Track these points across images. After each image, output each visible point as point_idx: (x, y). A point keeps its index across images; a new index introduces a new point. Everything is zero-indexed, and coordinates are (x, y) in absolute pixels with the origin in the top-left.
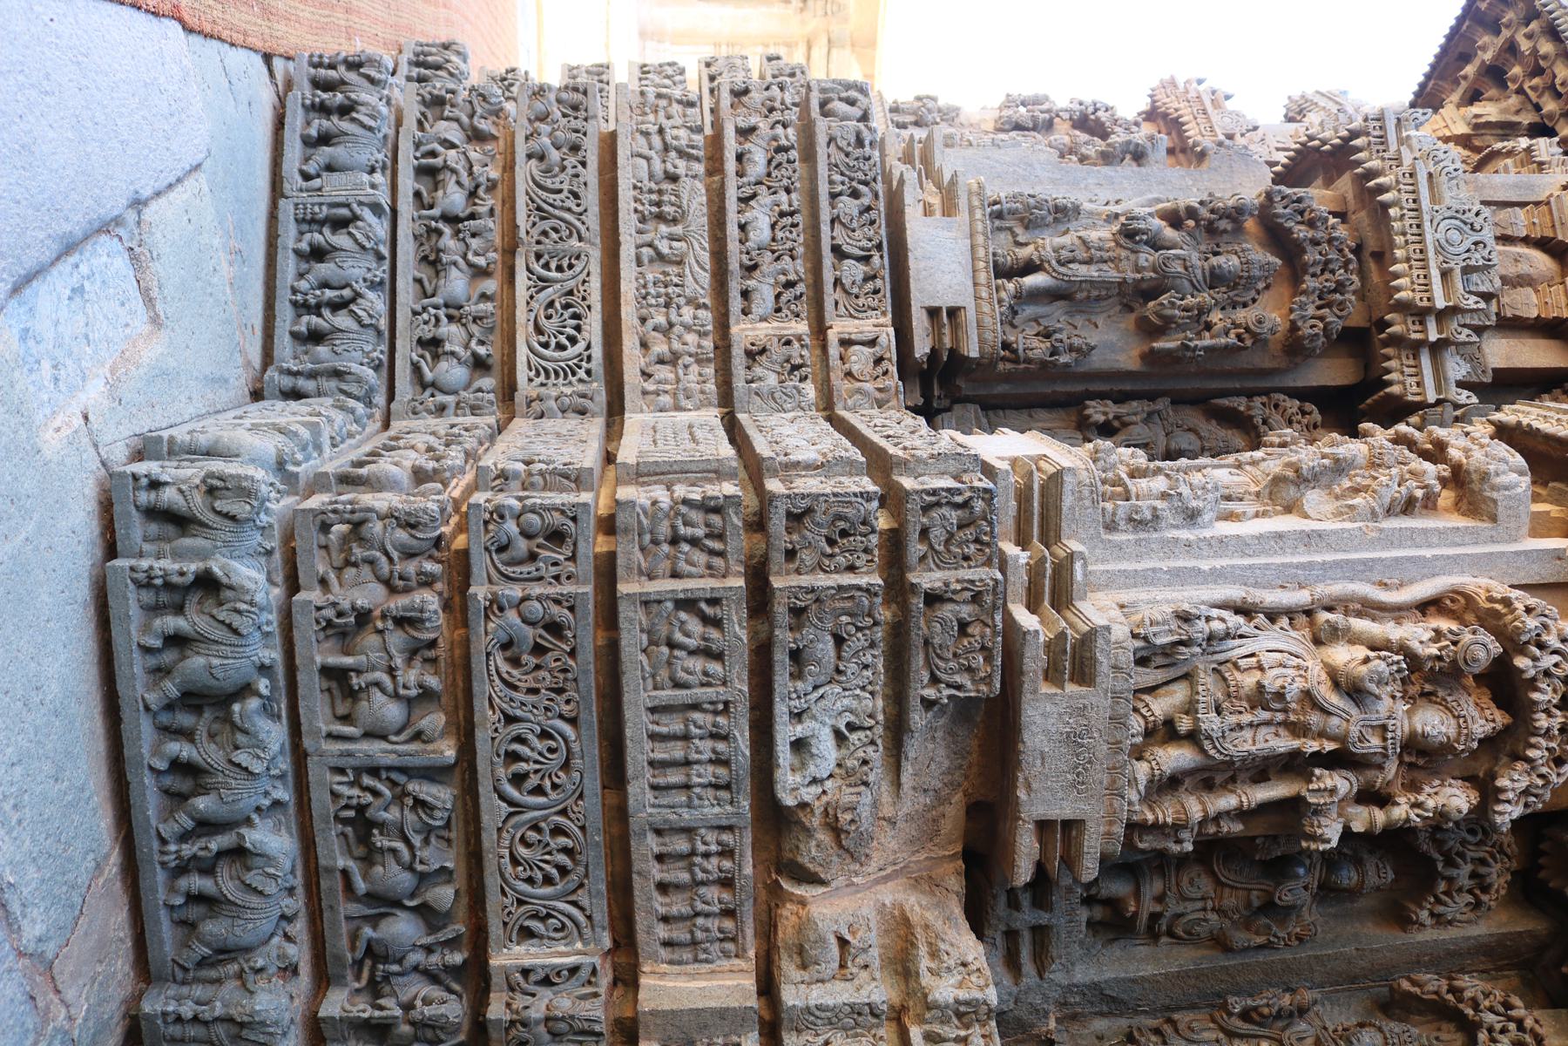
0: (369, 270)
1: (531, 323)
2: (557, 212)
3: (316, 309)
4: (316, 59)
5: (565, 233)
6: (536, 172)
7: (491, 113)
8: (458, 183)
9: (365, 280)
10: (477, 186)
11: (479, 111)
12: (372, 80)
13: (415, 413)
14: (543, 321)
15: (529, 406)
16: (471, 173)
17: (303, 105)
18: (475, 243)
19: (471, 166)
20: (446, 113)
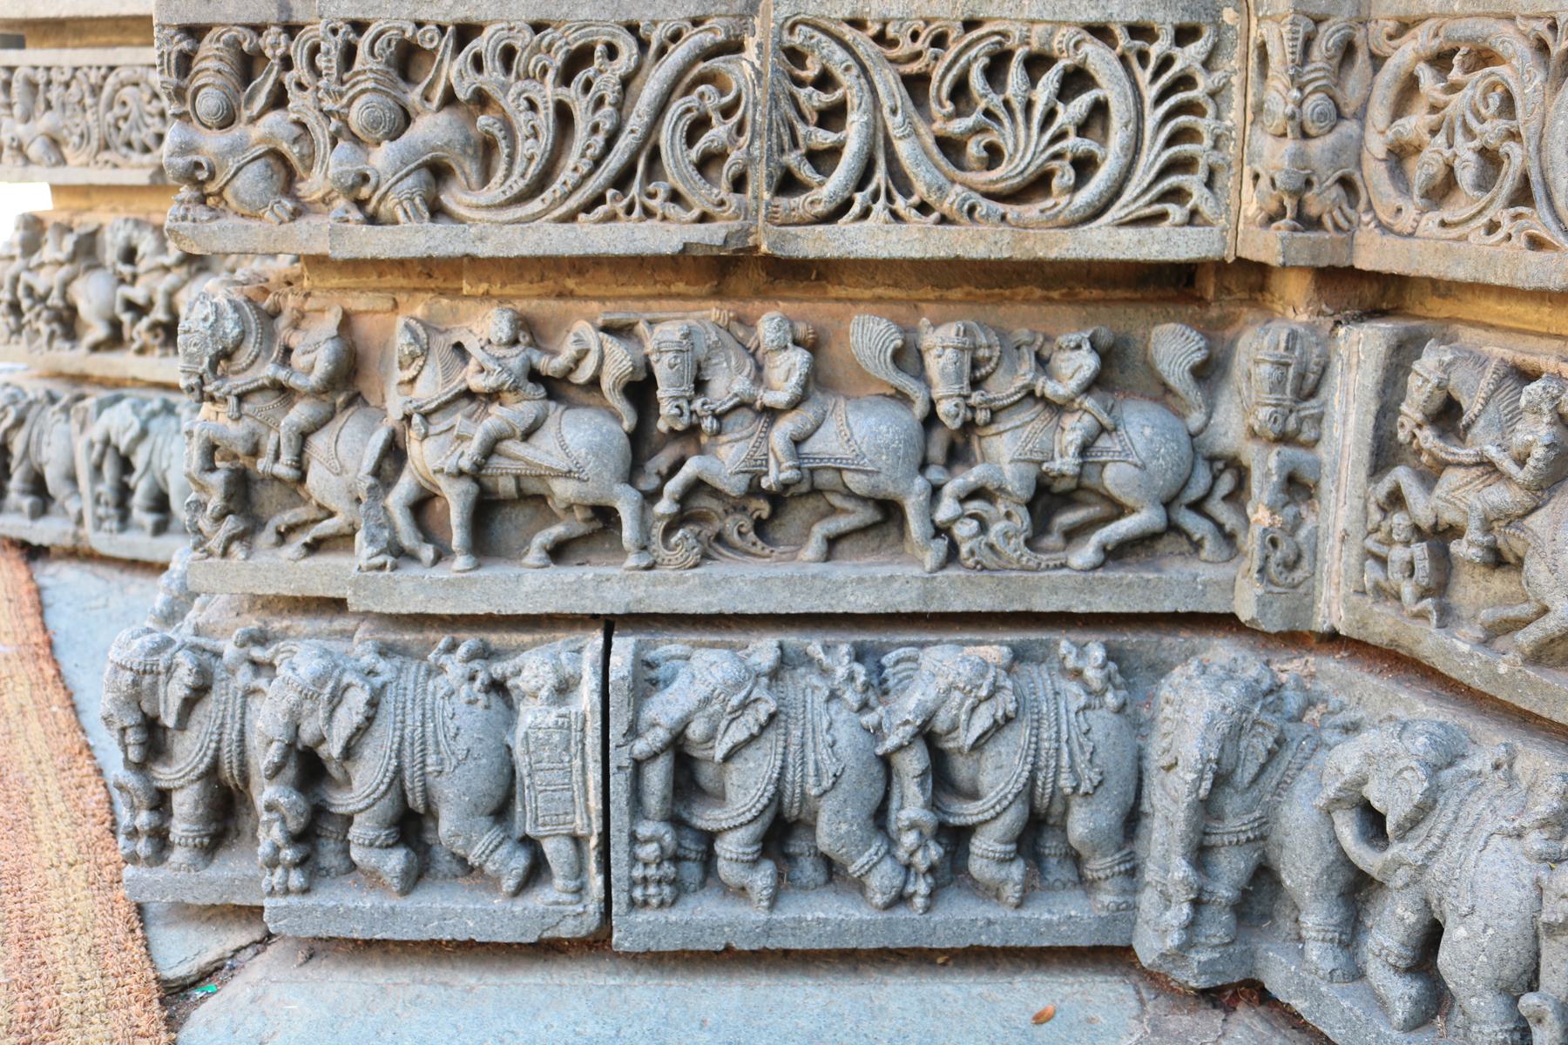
0: (833, 695)
1: (1012, 211)
2: (637, 121)
3: (956, 838)
4: (143, 847)
5: (711, 99)
6: (495, 191)
7: (268, 335)
8: (527, 435)
9: (864, 707)
10: (534, 375)
11: (268, 371)
12: (199, 692)
13: (1291, 565)
14: (1007, 174)
15: (1315, 224)
16: (493, 396)
17: (305, 891)
18: (727, 384)
19: (469, 394)
20: (283, 469)
